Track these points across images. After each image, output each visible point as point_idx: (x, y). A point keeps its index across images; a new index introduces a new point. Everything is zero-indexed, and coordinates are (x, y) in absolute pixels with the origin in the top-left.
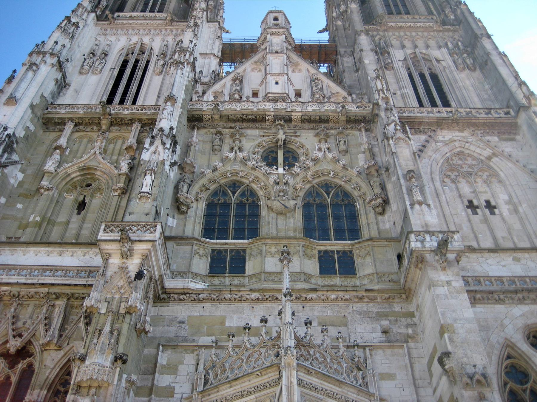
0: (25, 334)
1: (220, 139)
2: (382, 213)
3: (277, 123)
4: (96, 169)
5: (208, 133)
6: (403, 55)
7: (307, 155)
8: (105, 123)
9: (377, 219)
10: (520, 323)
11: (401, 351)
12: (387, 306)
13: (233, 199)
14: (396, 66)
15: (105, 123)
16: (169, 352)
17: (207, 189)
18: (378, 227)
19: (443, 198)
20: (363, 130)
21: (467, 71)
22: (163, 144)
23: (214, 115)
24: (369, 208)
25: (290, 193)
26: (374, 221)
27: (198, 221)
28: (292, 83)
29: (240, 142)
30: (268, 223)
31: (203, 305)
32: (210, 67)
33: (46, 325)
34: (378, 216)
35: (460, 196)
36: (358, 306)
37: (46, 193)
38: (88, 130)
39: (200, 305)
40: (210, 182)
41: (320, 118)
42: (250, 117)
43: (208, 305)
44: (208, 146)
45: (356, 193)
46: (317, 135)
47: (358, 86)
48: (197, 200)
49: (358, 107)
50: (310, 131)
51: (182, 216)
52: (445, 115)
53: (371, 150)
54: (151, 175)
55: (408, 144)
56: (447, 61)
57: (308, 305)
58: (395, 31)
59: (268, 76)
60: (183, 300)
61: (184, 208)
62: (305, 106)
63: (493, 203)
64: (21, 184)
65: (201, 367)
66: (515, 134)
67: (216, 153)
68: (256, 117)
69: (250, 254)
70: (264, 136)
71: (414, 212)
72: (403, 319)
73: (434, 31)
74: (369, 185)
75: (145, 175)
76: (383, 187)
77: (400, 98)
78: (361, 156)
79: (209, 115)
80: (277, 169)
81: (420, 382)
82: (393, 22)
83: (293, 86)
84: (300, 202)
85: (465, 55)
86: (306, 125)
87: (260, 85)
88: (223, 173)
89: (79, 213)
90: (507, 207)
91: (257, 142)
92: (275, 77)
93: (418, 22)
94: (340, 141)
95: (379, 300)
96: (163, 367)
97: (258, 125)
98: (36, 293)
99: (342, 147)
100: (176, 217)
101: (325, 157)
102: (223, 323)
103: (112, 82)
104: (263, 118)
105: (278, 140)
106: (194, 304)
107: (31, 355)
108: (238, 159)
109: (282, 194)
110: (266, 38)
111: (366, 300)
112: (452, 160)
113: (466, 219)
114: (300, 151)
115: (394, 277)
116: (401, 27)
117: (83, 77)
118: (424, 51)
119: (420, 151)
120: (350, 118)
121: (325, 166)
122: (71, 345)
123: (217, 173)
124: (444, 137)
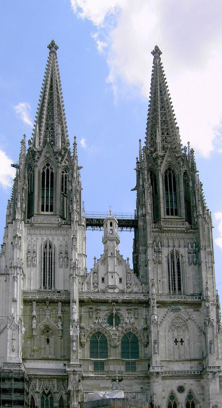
4: (49, 326)
6: (168, 252)
8: (47, 303)
12: (143, 380)
14: (163, 261)
15: (47, 303)
17: (89, 336)
18: (144, 352)
19: (167, 340)
21: (193, 265)
26: (143, 350)
30: (111, 350)
35: (173, 337)
36: (135, 381)
37: (36, 337)
38: (41, 305)
43: (95, 380)
45: (139, 339)
46: (127, 310)
47: (146, 276)
49: (144, 295)
51: (83, 348)
52: (176, 300)
56: (186, 259)
58: (167, 232)
60: (88, 379)
63: (183, 340)
64: (25, 332)
70: (108, 310)
72: (147, 384)
73: (185, 233)
75: (73, 342)
76: (148, 337)
77: (161, 284)
78: (142, 320)
82: (167, 227)
85: (194, 254)
89: (48, 344)
90: (187, 342)
93: (178, 228)
94: (135, 313)
95: (141, 379)
98: (47, 377)
99: (136, 316)
102: (99, 386)
107: (51, 393)
109: (115, 340)
112: (175, 320)
113: (172, 347)
114: (121, 318)
115: (146, 372)
117: (30, 268)
118: (177, 249)
119: (164, 317)
121: (129, 326)
122: (61, 392)
123: (92, 330)
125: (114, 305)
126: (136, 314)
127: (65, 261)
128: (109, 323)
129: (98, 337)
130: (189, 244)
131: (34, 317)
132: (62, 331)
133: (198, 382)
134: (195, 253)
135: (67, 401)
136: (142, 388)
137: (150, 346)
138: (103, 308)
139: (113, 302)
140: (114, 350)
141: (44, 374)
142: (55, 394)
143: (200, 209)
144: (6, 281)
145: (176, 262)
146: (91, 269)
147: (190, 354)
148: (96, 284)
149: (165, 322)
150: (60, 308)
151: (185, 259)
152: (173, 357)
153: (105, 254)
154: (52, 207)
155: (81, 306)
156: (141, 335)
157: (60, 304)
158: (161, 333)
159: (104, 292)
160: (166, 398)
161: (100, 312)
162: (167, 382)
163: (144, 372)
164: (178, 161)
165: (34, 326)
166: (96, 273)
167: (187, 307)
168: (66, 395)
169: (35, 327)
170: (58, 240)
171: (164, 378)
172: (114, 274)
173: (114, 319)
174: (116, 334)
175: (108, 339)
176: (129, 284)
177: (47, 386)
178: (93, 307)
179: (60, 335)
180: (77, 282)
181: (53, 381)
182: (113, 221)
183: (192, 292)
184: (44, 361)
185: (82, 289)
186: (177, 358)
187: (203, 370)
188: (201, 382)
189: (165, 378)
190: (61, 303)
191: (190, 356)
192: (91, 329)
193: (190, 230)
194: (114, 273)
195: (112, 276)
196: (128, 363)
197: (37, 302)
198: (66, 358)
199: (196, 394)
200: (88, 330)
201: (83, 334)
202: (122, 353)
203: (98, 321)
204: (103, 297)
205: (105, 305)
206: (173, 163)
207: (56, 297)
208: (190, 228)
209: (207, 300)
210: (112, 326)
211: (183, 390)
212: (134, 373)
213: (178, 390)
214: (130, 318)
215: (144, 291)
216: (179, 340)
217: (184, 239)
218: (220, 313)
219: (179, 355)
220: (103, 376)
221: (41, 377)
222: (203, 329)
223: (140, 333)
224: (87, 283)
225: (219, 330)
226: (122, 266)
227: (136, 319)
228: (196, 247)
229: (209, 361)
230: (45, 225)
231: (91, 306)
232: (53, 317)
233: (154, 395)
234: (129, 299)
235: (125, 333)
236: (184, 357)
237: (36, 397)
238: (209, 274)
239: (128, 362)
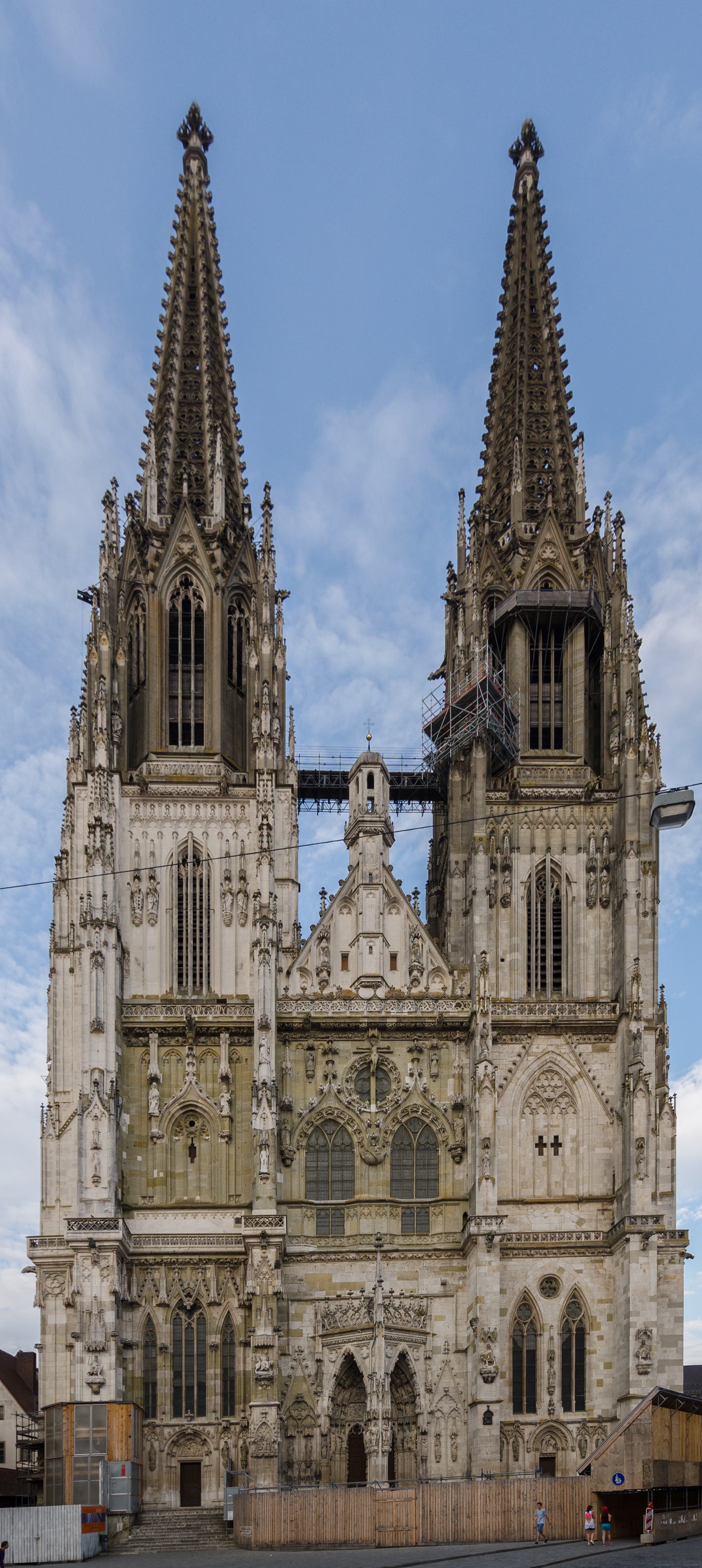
0: (194, 1295)
1: (313, 1060)
2: (458, 1163)
5: (300, 1047)
8: (190, 1034)
9: (453, 1169)
10: (539, 1274)
11: (451, 1299)
12: (448, 1261)
16: (296, 1304)
24: (449, 1156)
25: (381, 1139)
26: (451, 1171)
29: (333, 1062)
31: (315, 1264)
33: (205, 1286)
36: (428, 1263)
39: (312, 1265)
43: (318, 1265)
44: (301, 1069)
45: (440, 1138)
46: (410, 1051)
51: (288, 1170)
53: (461, 1077)
57: (391, 1262)
61: (288, 1162)
65: (319, 1317)
66: (611, 1041)
67: (310, 1080)
69: (349, 1216)
70: (355, 1053)
72: (457, 1273)
78: (451, 1081)
81: (459, 1322)
82: (529, 787)
84: (388, 1150)
85: (605, 871)
86: (399, 1035)
87: (352, 945)
91: (349, 1063)
93: (562, 787)
95: (443, 1257)
96: (293, 1316)
99: (434, 1070)
101: (415, 1086)
102: (330, 1280)
103: (176, 941)
106: (309, 1264)
107: (200, 1308)
108: (333, 1093)
110: (357, 837)
111: (434, 1257)
116: (538, 797)
119: (510, 1071)
123: (313, 1114)
124: (537, 1048)
126: (435, 1062)
127: (240, 903)
128: (358, 1093)
130: (592, 841)
131: (154, 1079)
132: (231, 1119)
133: (598, 1264)
134: (607, 868)
135: (242, 1327)
136: (444, 1284)
137: (469, 1159)
138: (345, 1045)
139: (373, 1028)
140: (372, 1172)
141: (182, 1250)
142: (211, 1308)
143: (629, 722)
144: (72, 971)
145: (550, 900)
146: (313, 928)
147: (578, 1183)
149: (512, 1085)
150: (223, 1051)
151: (578, 891)
152: (531, 1190)
153: (351, 879)
154: (199, 727)
155: (284, 1043)
157: (224, 1036)
158: (501, 1120)
159: (347, 998)
160: (509, 1312)
161: (336, 1059)
162: (515, 1264)
163: (451, 1238)
164: (573, 559)
165: (154, 1108)
167: (575, 1038)
168: (240, 1310)
169: (157, 1111)
170: (221, 834)
171: (506, 1252)
173: (373, 1080)
174: (378, 1126)
175: (355, 1139)
176: (415, 973)
177: (189, 1284)
178: (316, 1043)
179: (226, 1132)
180: (273, 970)
181: (205, 1269)
182: (377, 772)
183: (590, 994)
184: (182, 1211)
185: (286, 989)
186: (541, 1193)
187: (611, 1230)
188: (605, 1265)
189: (507, 1255)
190: (227, 1035)
191: (578, 1188)
193: (597, 795)
195: (371, 948)
196: (408, 1211)
197: (161, 1035)
198: (243, 1201)
199: (589, 1301)
200: (301, 1114)
201: (289, 1128)
202: (392, 1180)
203: (330, 1087)
205: (348, 1039)
206: (560, 567)
207: (215, 1017)
208: (597, 787)
209: (635, 1014)
210: (367, 1102)
211: (555, 1289)
212: (423, 1241)
213: (543, 1289)
215: (458, 992)
216: (548, 1140)
217: (578, 824)
218: (668, 1057)
219: (549, 1185)
220: (341, 1252)
221: (174, 1258)
222: (617, 1106)
223: (444, 1121)
225: (661, 1109)
227: (435, 1076)
228: (611, 849)
229: (632, 1199)
230: (180, 786)
231: (311, 1042)
232: (206, 1081)
233: (477, 1303)
235: (404, 1120)
236: (561, 1190)
237: (161, 1321)
238: (644, 937)
239: (408, 1208)
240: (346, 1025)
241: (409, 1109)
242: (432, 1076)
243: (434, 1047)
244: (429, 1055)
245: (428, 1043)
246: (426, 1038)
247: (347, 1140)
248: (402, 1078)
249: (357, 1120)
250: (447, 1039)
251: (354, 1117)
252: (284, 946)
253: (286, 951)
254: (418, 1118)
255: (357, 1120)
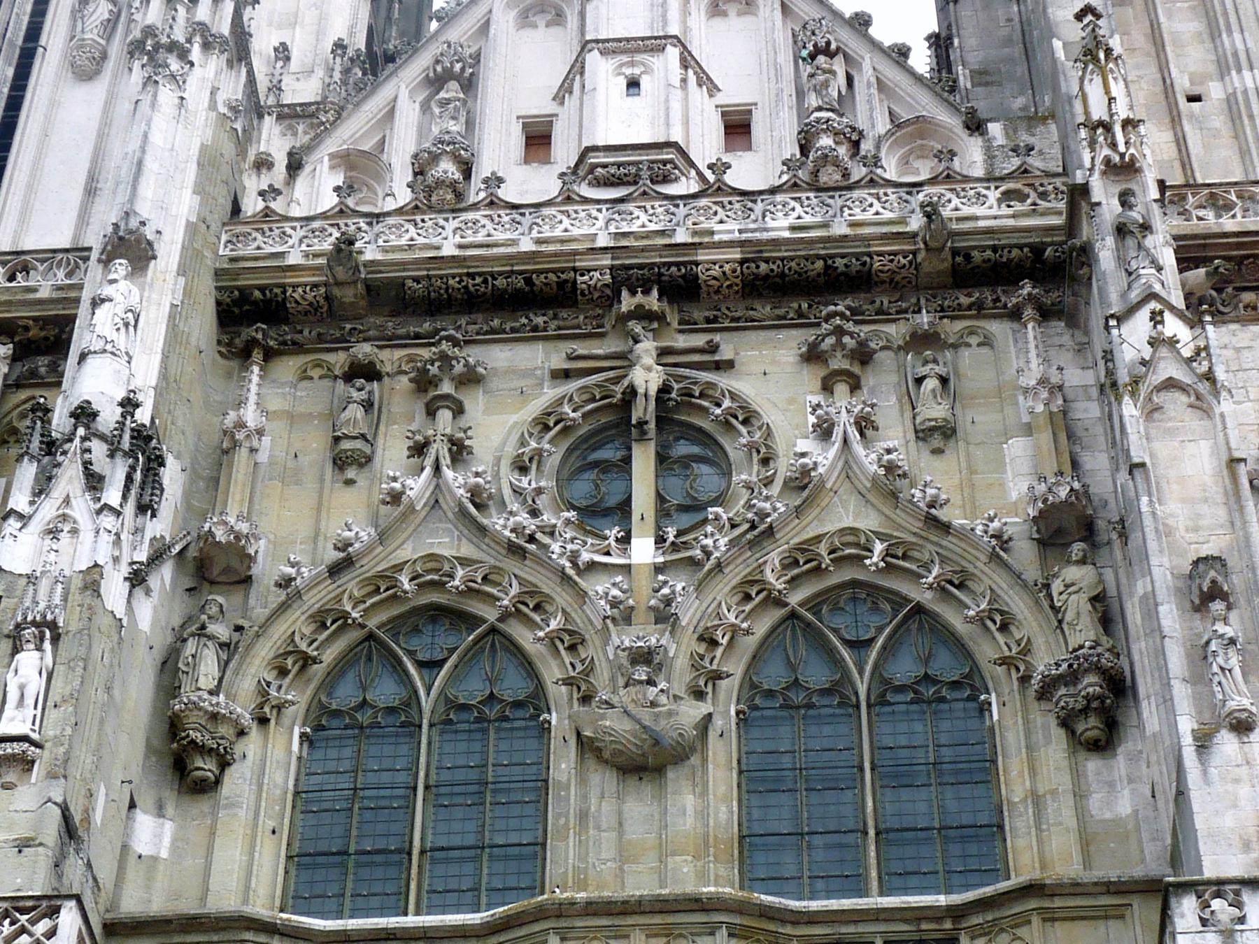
1: (368, 405)
2: (1103, 744)
3: (627, 302)
5: (315, 373)
7: (765, 461)
13: (427, 703)
17: (306, 661)
20: (1029, 312)
22: (94, 482)
23: (338, 284)
26: (1063, 781)
27: (271, 824)
28: (706, 81)
29: (458, 410)
30: (583, 816)
32: (322, 20)
34: (1082, 755)
40: (323, 626)
41: (827, 267)
42: (501, 283)
44: (315, 444)
45: (987, 651)
48: (263, 721)
50: (782, 335)
54: (39, 648)
55: (1207, 413)
59: (594, 59)
61: (205, 766)
62: (759, 207)
67: (351, 473)
68: (529, 281)
70: (566, 375)
71: (1213, 771)
74: (1046, 604)
75: (16, 650)
77: (1219, 122)
79: (315, 286)
80: (625, 540)
83: (713, 89)
86: (764, 310)
87: (559, 98)
88: (381, 576)
92: (625, 58)
94: (919, 381)
97: (540, 320)
99: (935, 411)
100: (170, 810)
104: (561, 284)
105: (632, 392)
108: (448, 505)
109: (641, 673)
114: (734, 448)
120: (968, 257)
123: (351, 583)
125: (642, 314)
126: (931, 384)
129: (430, 666)
148: (447, 169)
156: (1018, 604)
161: (475, 402)
166: (453, 85)
172: (655, 61)
173: (643, 462)
175: (552, 672)
176: (826, 141)
178: (389, 359)
192: (335, 570)
194: (654, 44)
195: (633, 84)
204: (514, 242)
205: (536, 335)
214: (844, 422)
223: (1001, 581)
224: (347, 160)
226: (747, 20)
234: (828, 240)
240: (520, 283)
241: (823, 549)
242: (923, 434)
243: (922, 341)
244: (902, 368)
245: (895, 331)
246: (882, 315)
247: (513, 686)
248: (780, 445)
249: (562, 598)
250: (979, 309)
251: (547, 585)
252: (287, 99)
253: (290, 115)
254: (873, 591)
255: (562, 598)
